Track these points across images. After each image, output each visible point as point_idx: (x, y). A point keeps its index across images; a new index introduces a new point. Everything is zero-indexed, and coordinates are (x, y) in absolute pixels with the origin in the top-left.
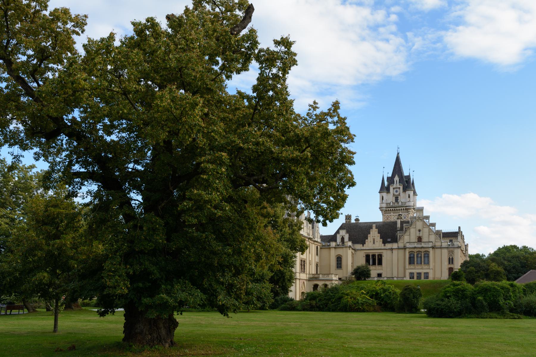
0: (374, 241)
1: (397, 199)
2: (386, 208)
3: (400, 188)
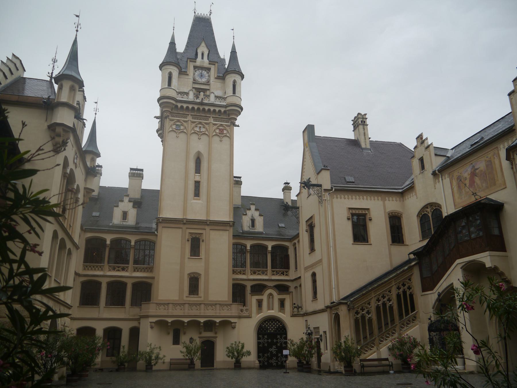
2: (177, 101)
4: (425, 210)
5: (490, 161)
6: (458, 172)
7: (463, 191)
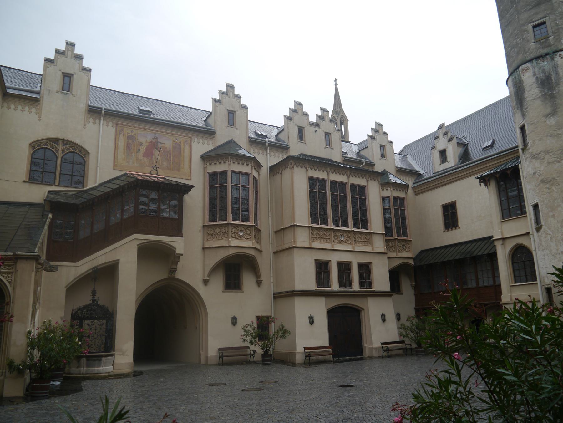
4: (50, 144)
5: (180, 146)
6: (132, 131)
7: (133, 154)
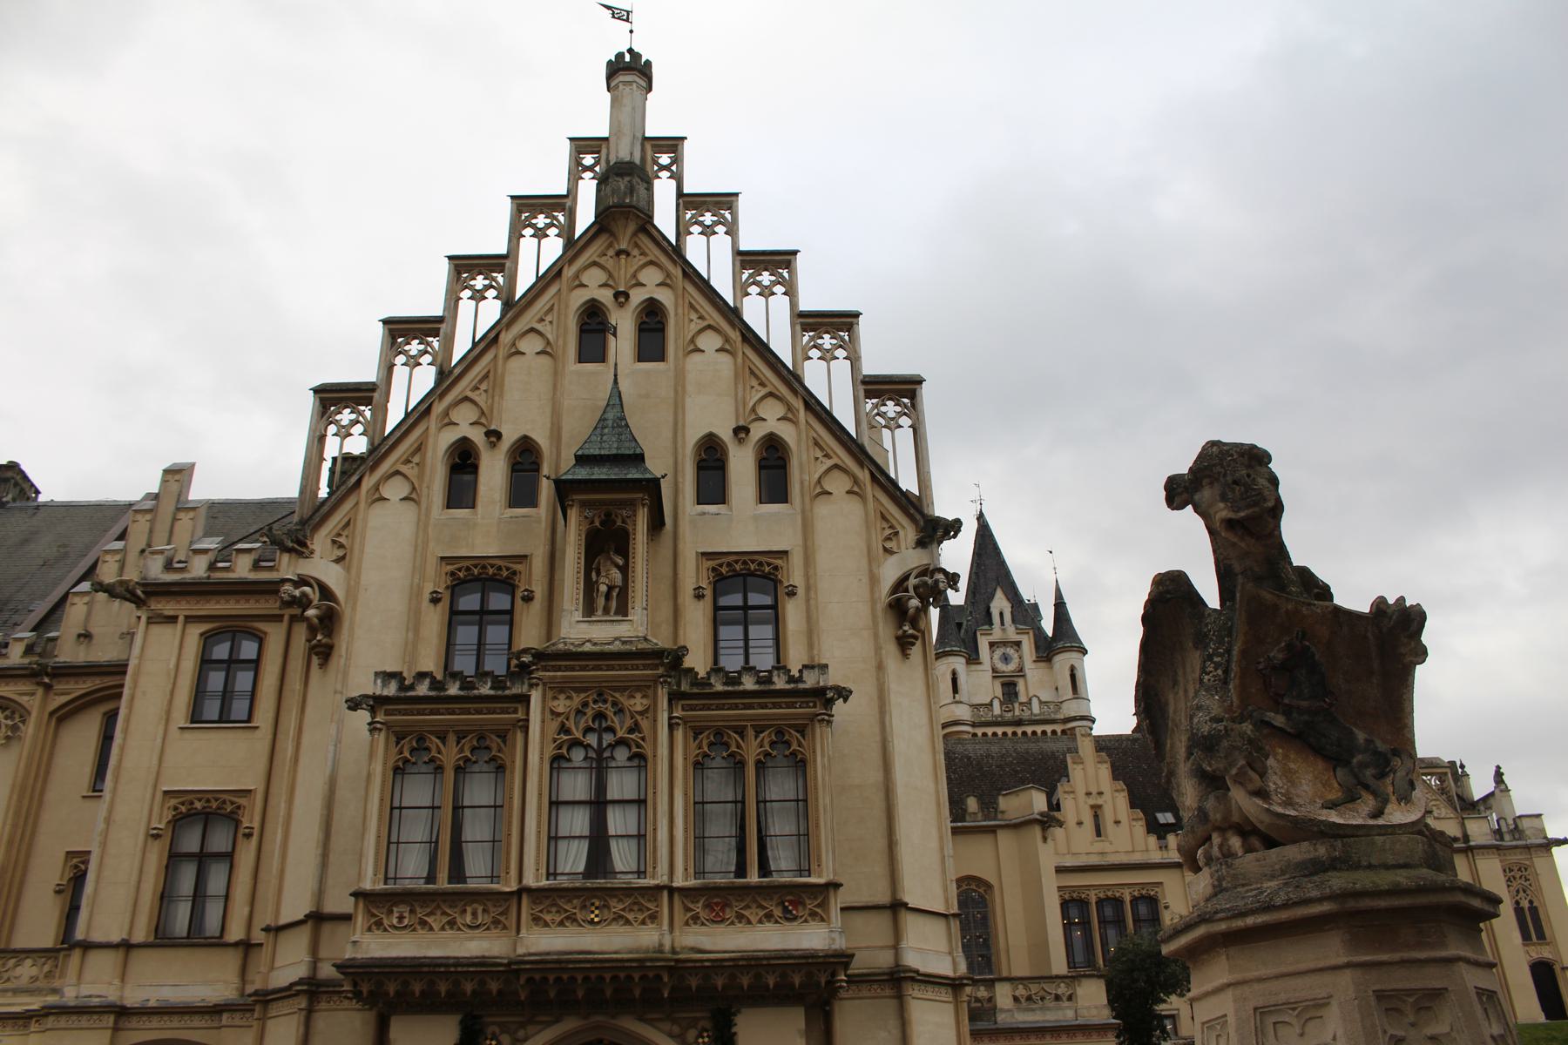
0: (1096, 817)
1: (1009, 690)
3: (1018, 644)
